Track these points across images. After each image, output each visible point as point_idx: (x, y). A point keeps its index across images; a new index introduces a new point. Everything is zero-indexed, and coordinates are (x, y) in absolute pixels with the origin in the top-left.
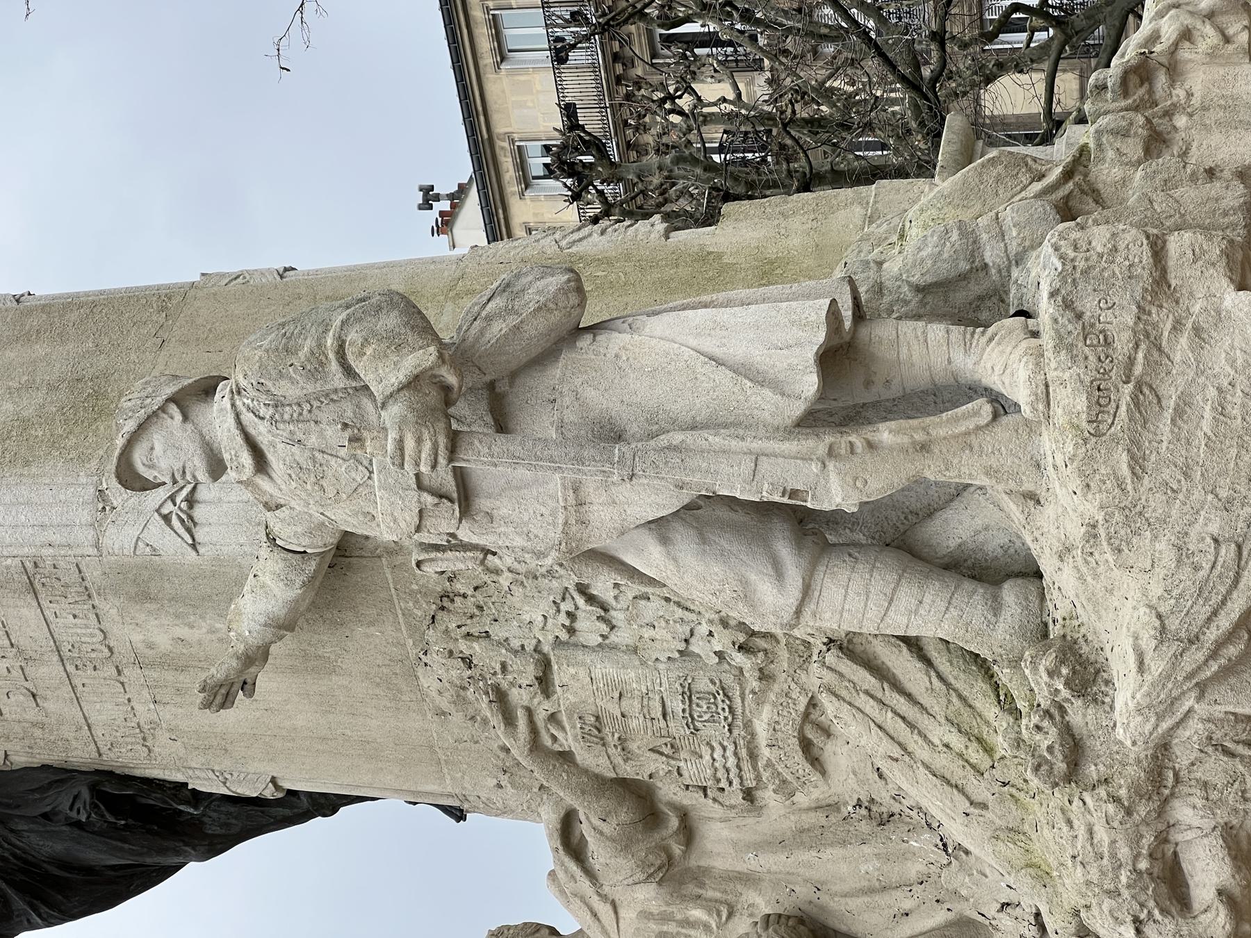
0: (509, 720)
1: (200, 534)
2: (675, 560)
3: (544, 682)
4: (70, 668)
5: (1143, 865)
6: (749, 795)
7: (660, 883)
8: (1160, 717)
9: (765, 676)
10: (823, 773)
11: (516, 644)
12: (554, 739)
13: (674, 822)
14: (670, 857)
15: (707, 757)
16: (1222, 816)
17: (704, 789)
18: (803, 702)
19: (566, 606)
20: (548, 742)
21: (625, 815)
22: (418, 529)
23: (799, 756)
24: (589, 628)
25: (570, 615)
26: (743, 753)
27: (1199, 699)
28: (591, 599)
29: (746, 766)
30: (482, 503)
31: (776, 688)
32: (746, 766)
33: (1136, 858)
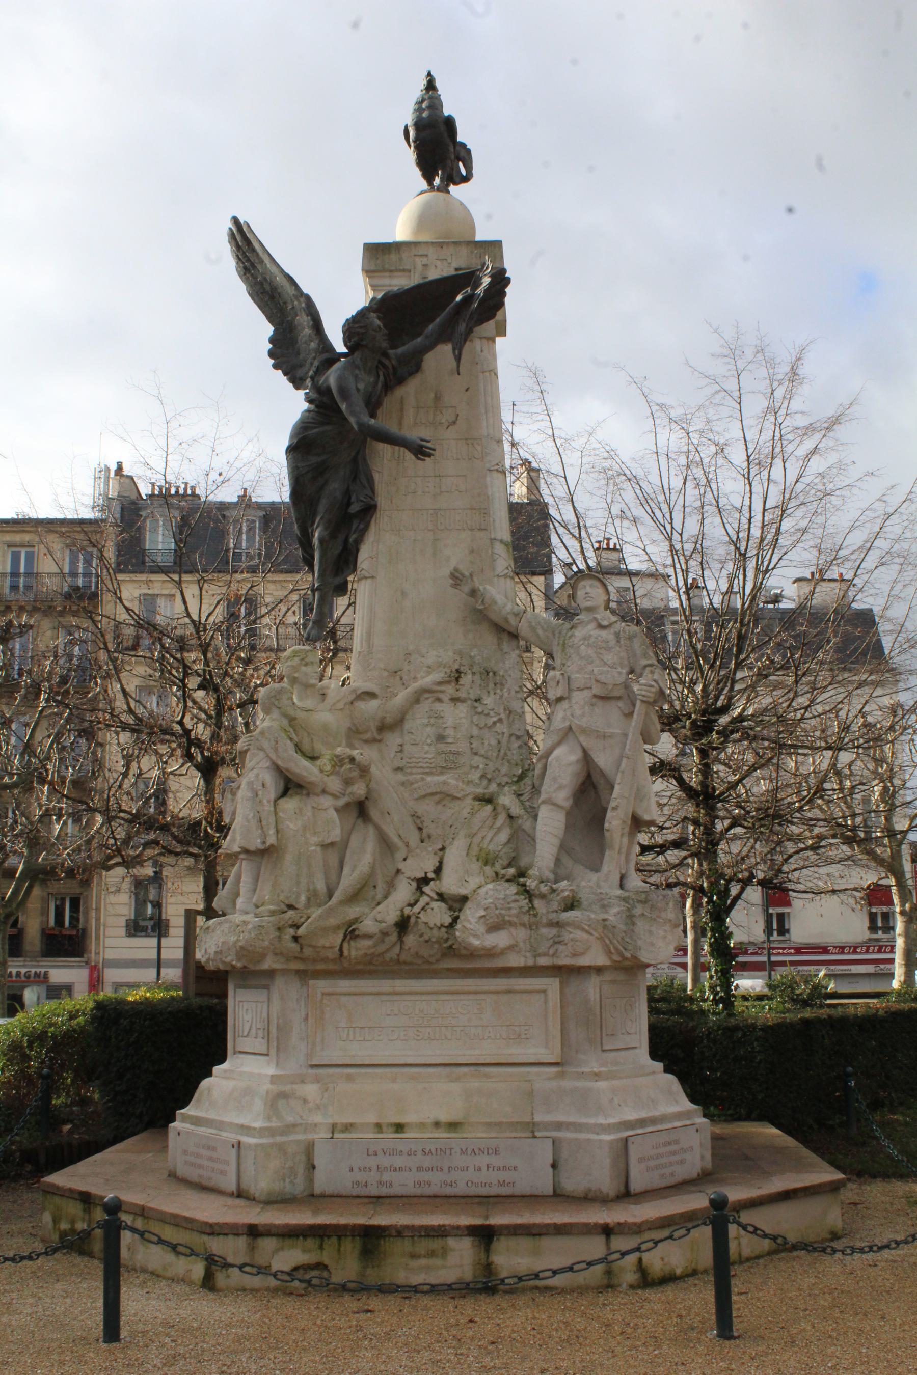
0: (440, 683)
1: (502, 579)
2: (570, 764)
3: (455, 700)
4: (431, 512)
5: (507, 918)
6: (399, 769)
7: (349, 728)
8: (589, 926)
9: (469, 782)
10: (417, 799)
11: (471, 691)
12: (427, 698)
13: (378, 737)
14: (361, 733)
15: (426, 756)
16: (521, 945)
17: (401, 751)
18: (459, 796)
19: (492, 713)
20: (426, 695)
21: (389, 720)
22: (597, 681)
23: (430, 791)
24: (483, 721)
25: (488, 715)
26: (428, 770)
27: (597, 938)
28: (495, 723)
29: (421, 770)
30: (600, 703)
31: (464, 786)
32: (421, 770)
33: (509, 916)
